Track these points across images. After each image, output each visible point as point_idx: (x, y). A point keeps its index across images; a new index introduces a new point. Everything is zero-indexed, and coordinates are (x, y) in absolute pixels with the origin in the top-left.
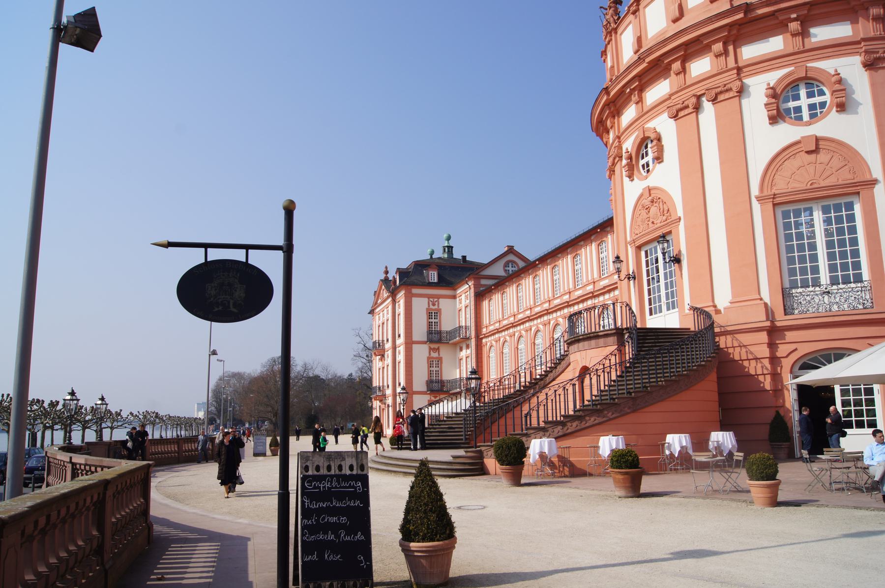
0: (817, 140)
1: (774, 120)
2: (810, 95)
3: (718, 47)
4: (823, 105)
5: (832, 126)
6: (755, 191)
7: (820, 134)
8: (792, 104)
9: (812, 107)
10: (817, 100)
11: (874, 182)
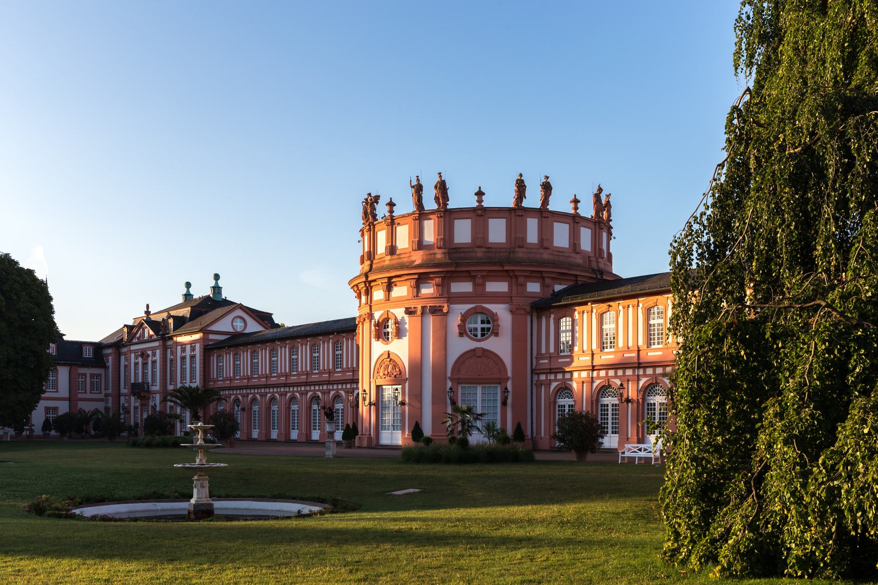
0: (484, 350)
1: (461, 334)
2: (483, 322)
3: (438, 280)
4: (489, 329)
5: (491, 344)
6: (449, 375)
7: (485, 347)
8: (473, 326)
9: (483, 329)
10: (486, 326)
11: (508, 379)
